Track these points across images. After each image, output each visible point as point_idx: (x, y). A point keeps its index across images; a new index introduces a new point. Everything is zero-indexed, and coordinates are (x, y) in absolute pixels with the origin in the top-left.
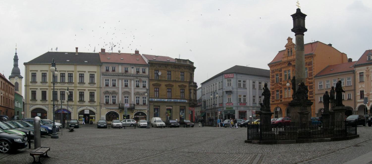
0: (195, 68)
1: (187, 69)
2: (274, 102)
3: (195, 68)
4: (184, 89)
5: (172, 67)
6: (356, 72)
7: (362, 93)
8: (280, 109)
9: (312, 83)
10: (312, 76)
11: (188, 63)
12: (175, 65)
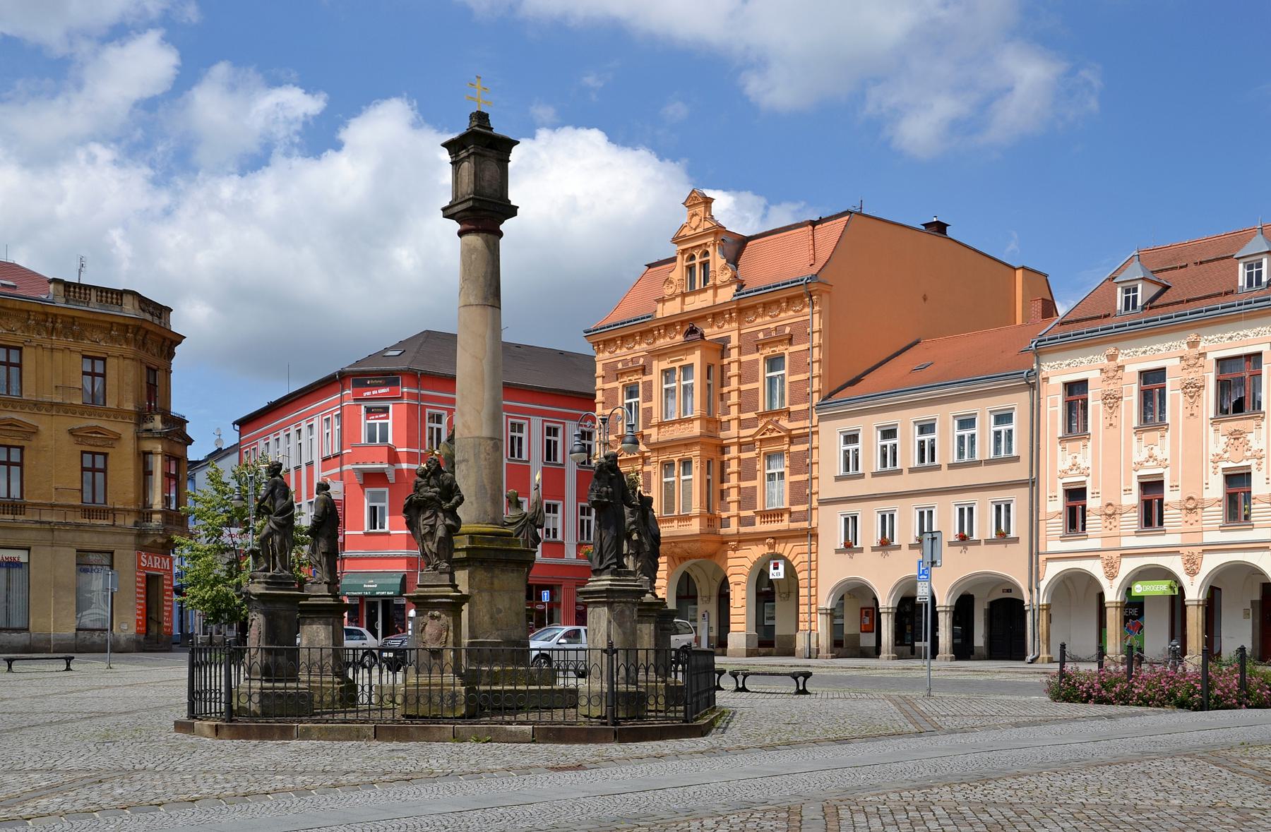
0: (179, 339)
1: (127, 341)
3: (179, 339)
4: (106, 450)
5: (32, 322)
7: (1076, 495)
9: (805, 437)
10: (807, 397)
11: (130, 309)
12: (46, 314)
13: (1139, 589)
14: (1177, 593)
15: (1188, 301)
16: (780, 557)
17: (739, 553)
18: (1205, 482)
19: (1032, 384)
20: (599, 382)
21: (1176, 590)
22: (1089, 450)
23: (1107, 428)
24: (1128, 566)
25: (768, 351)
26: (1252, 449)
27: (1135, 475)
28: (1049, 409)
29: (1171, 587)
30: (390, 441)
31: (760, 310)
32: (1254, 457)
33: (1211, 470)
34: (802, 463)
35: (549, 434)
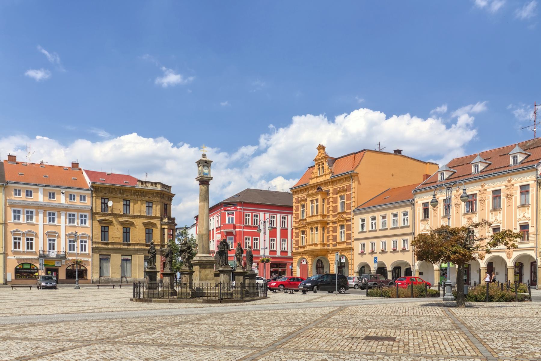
2: (336, 246)
8: (346, 259)
9: (350, 220)
10: (350, 208)
16: (344, 256)
17: (332, 255)
19: (413, 204)
20: (294, 204)
22: (477, 217)
25: (340, 194)
30: (234, 223)
31: (338, 181)
34: (349, 228)
35: (283, 219)
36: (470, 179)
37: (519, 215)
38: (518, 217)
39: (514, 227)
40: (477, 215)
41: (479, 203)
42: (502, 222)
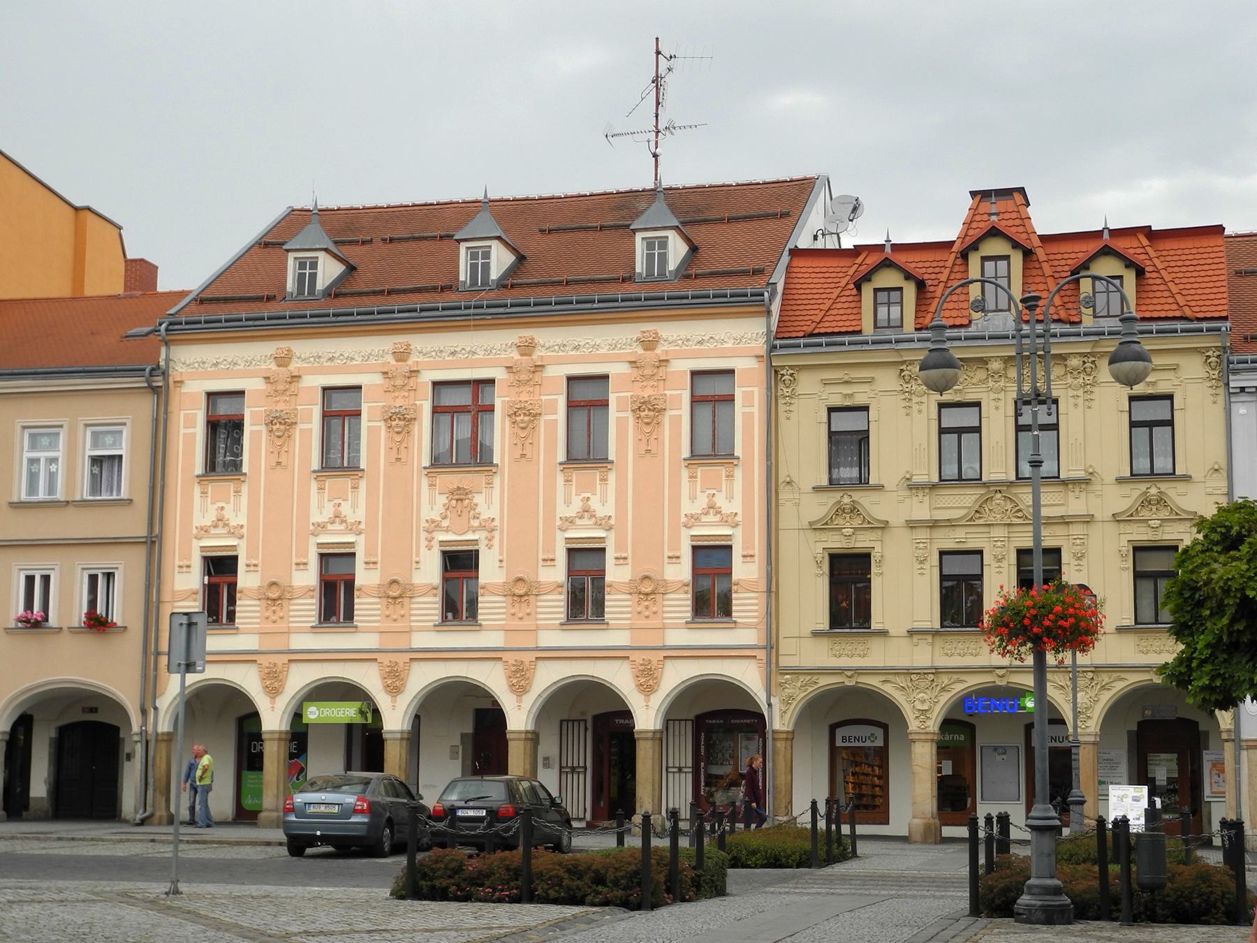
6: (180, 383)
13: (313, 713)
14: (370, 721)
15: (390, 292)
18: (415, 559)
21: (369, 716)
23: (273, 468)
24: (300, 678)
26: (482, 517)
27: (313, 541)
28: (182, 431)
29: (362, 712)
32: (482, 527)
33: (423, 543)
36: (467, 308)
37: (693, 498)
38: (687, 507)
39: (667, 553)
40: (497, 481)
41: (507, 424)
42: (612, 522)
